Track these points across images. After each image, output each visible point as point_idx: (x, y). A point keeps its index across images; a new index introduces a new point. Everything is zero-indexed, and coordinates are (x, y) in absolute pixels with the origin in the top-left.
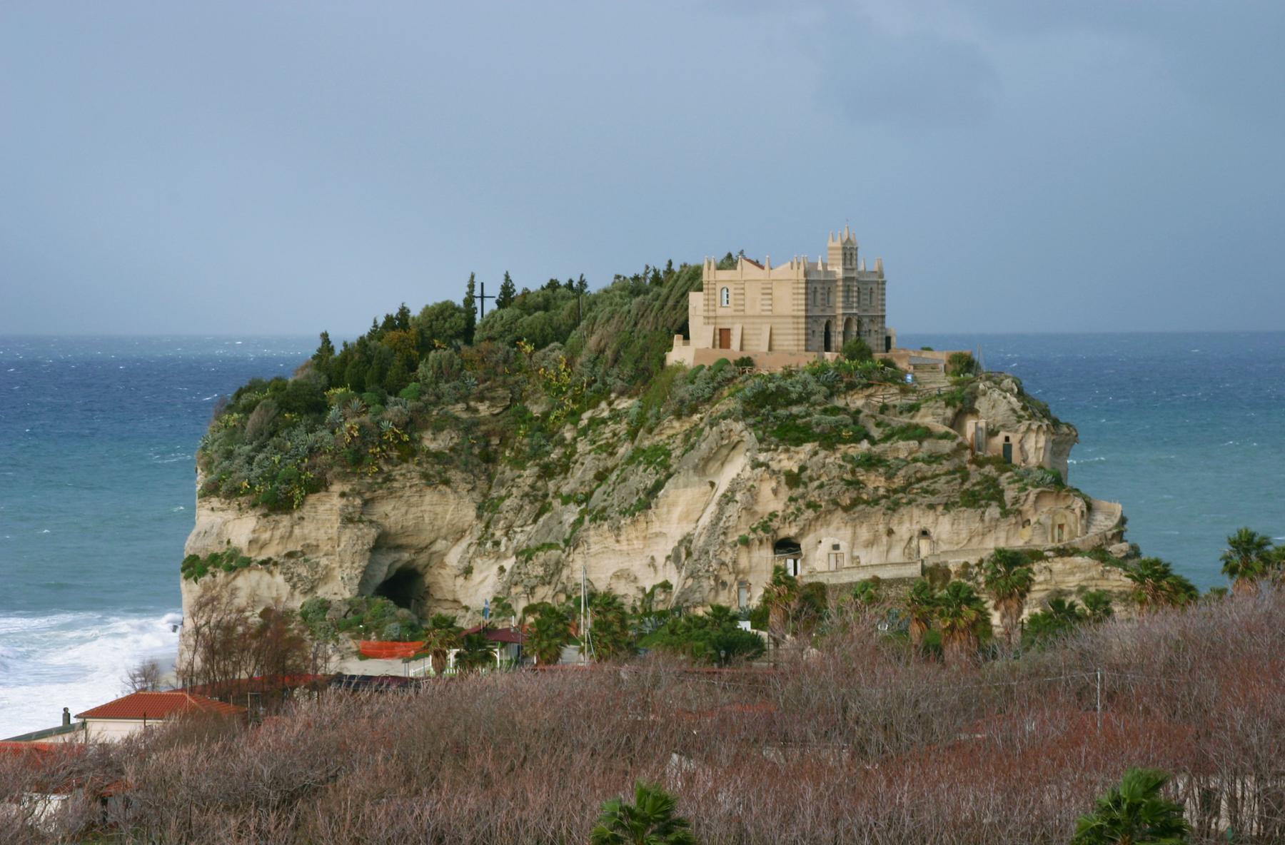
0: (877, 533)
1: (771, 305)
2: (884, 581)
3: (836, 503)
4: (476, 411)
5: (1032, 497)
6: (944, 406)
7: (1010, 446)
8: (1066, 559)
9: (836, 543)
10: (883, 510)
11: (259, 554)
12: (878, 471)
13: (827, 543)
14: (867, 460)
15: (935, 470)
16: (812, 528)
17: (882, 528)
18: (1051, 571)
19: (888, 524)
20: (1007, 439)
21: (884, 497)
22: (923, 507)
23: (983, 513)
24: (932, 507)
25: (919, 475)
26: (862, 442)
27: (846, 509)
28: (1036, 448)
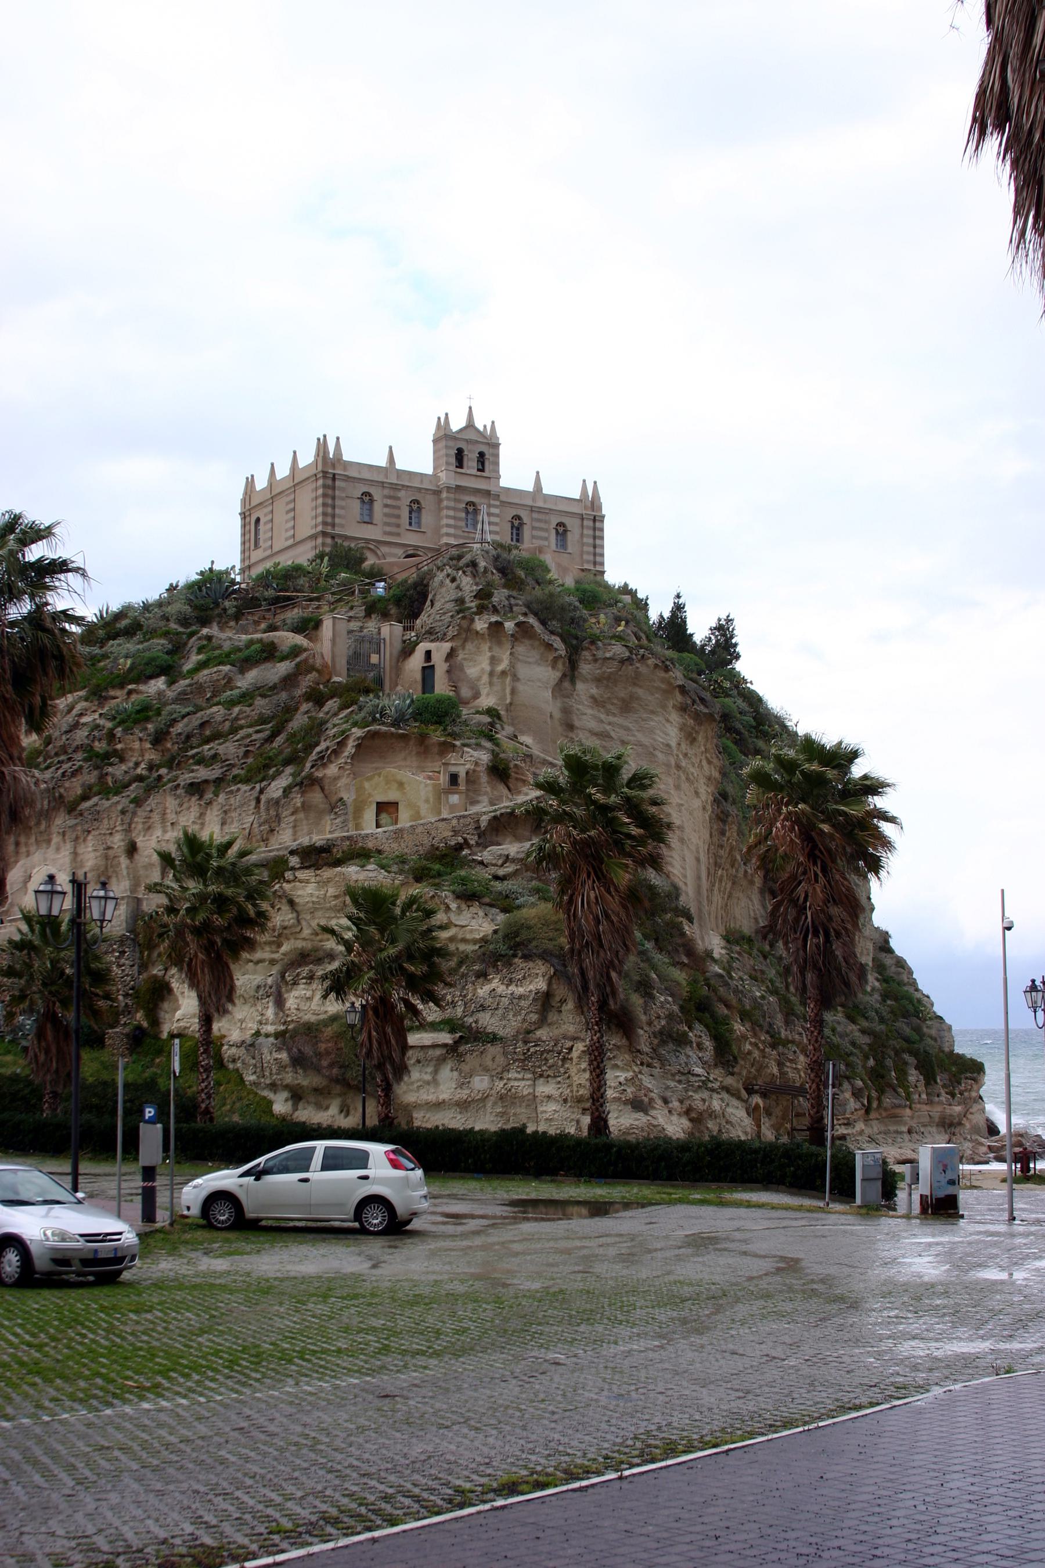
0: (111, 853)
5: (350, 748)
8: (327, 873)
10: (125, 802)
12: (146, 729)
14: (138, 712)
15: (237, 719)
16: (23, 849)
17: (118, 841)
18: (291, 903)
19: (128, 830)
20: (428, 654)
21: (140, 778)
22: (179, 792)
24: (196, 789)
26: (153, 682)
28: (491, 674)
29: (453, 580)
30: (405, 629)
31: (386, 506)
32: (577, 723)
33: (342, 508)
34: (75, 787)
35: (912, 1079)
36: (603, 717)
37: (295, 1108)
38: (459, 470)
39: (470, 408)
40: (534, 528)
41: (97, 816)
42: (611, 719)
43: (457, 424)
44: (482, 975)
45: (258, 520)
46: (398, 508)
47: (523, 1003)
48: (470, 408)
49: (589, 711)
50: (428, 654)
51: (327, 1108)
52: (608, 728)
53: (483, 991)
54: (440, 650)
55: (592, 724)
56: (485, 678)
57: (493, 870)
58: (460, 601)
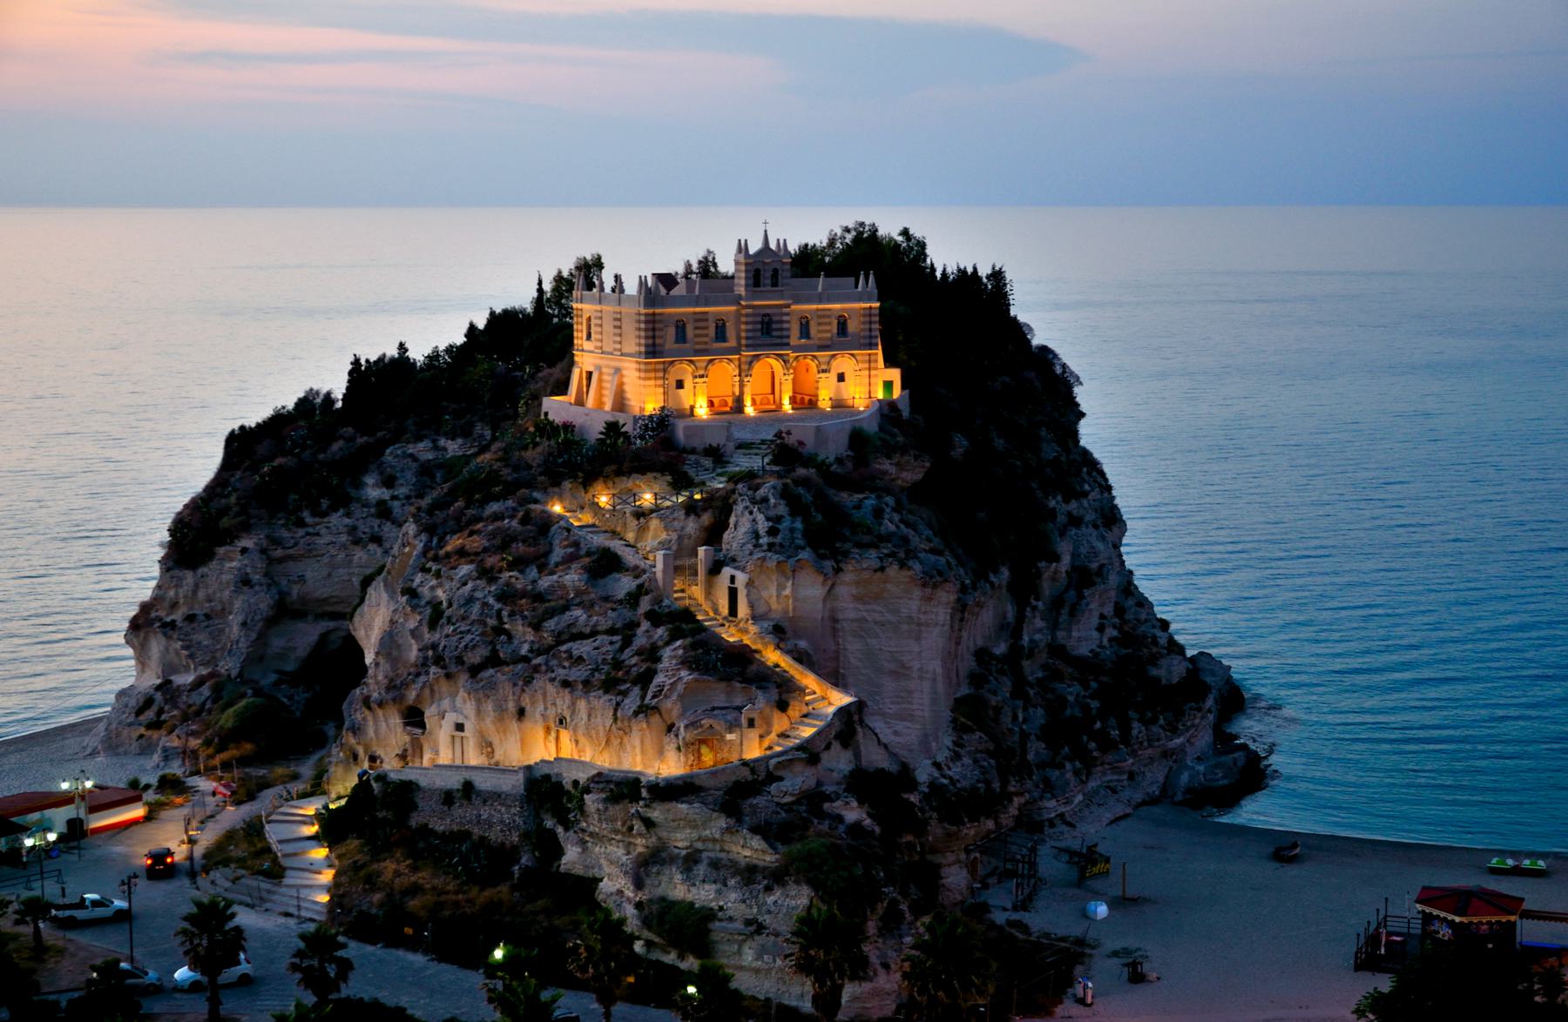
1: (620, 343)
2: (479, 793)
3: (460, 660)
4: (445, 449)
6: (683, 517)
7: (736, 589)
9: (460, 721)
11: (167, 615)
13: (451, 718)
15: (595, 625)
17: (511, 706)
20: (733, 579)
22: (556, 683)
23: (618, 704)
24: (566, 684)
25: (574, 631)
27: (474, 671)
29: (751, 513)
30: (716, 551)
31: (696, 328)
32: (840, 616)
33: (661, 337)
34: (475, 658)
35: (1135, 732)
36: (861, 607)
37: (648, 951)
38: (756, 289)
39: (766, 231)
40: (819, 324)
41: (492, 686)
42: (867, 607)
43: (755, 247)
44: (768, 889)
45: (589, 319)
46: (706, 328)
47: (795, 912)
48: (766, 231)
49: (851, 605)
50: (733, 579)
51: (669, 953)
52: (865, 614)
53: (770, 899)
54: (741, 578)
55: (852, 615)
56: (775, 599)
57: (776, 800)
58: (757, 536)
